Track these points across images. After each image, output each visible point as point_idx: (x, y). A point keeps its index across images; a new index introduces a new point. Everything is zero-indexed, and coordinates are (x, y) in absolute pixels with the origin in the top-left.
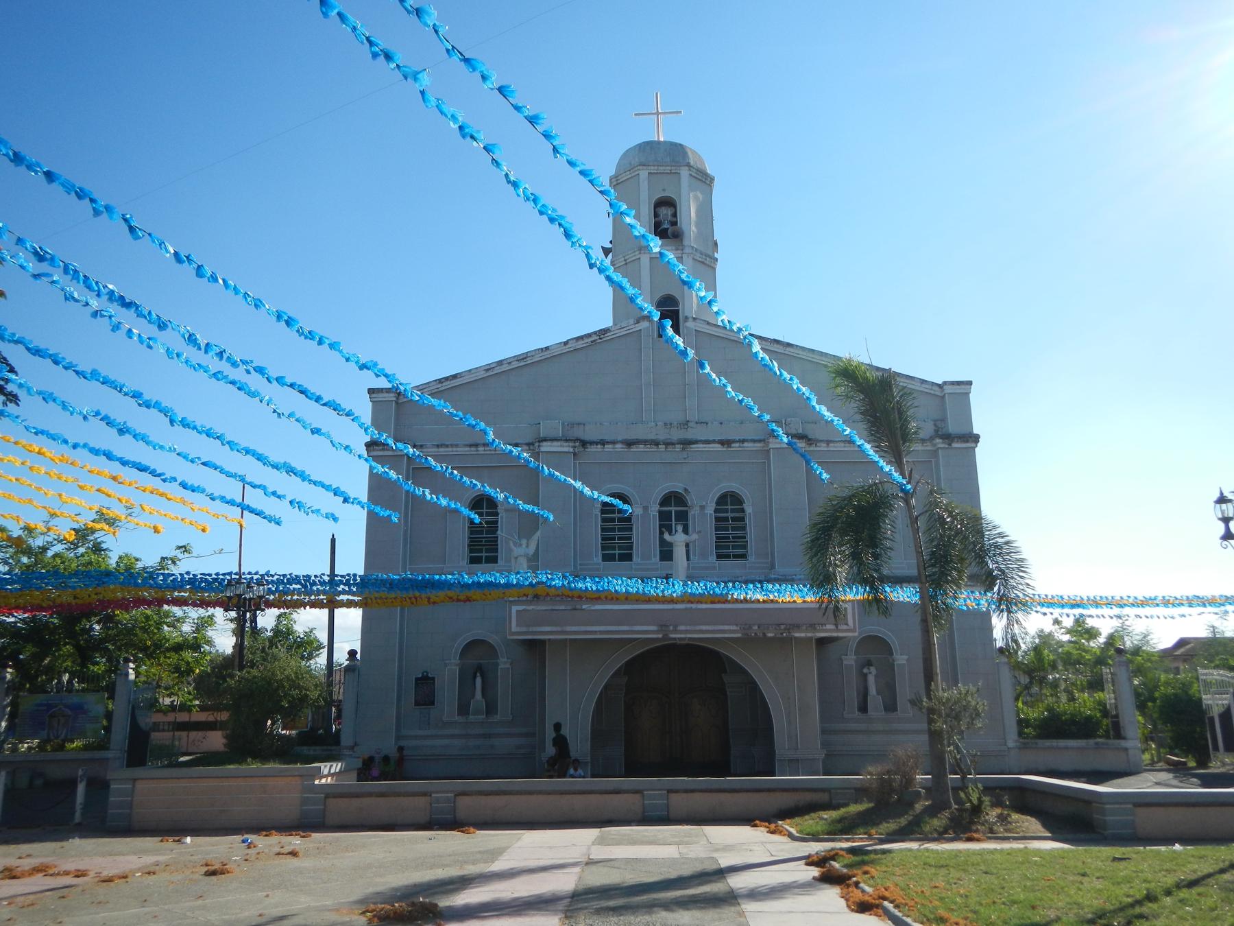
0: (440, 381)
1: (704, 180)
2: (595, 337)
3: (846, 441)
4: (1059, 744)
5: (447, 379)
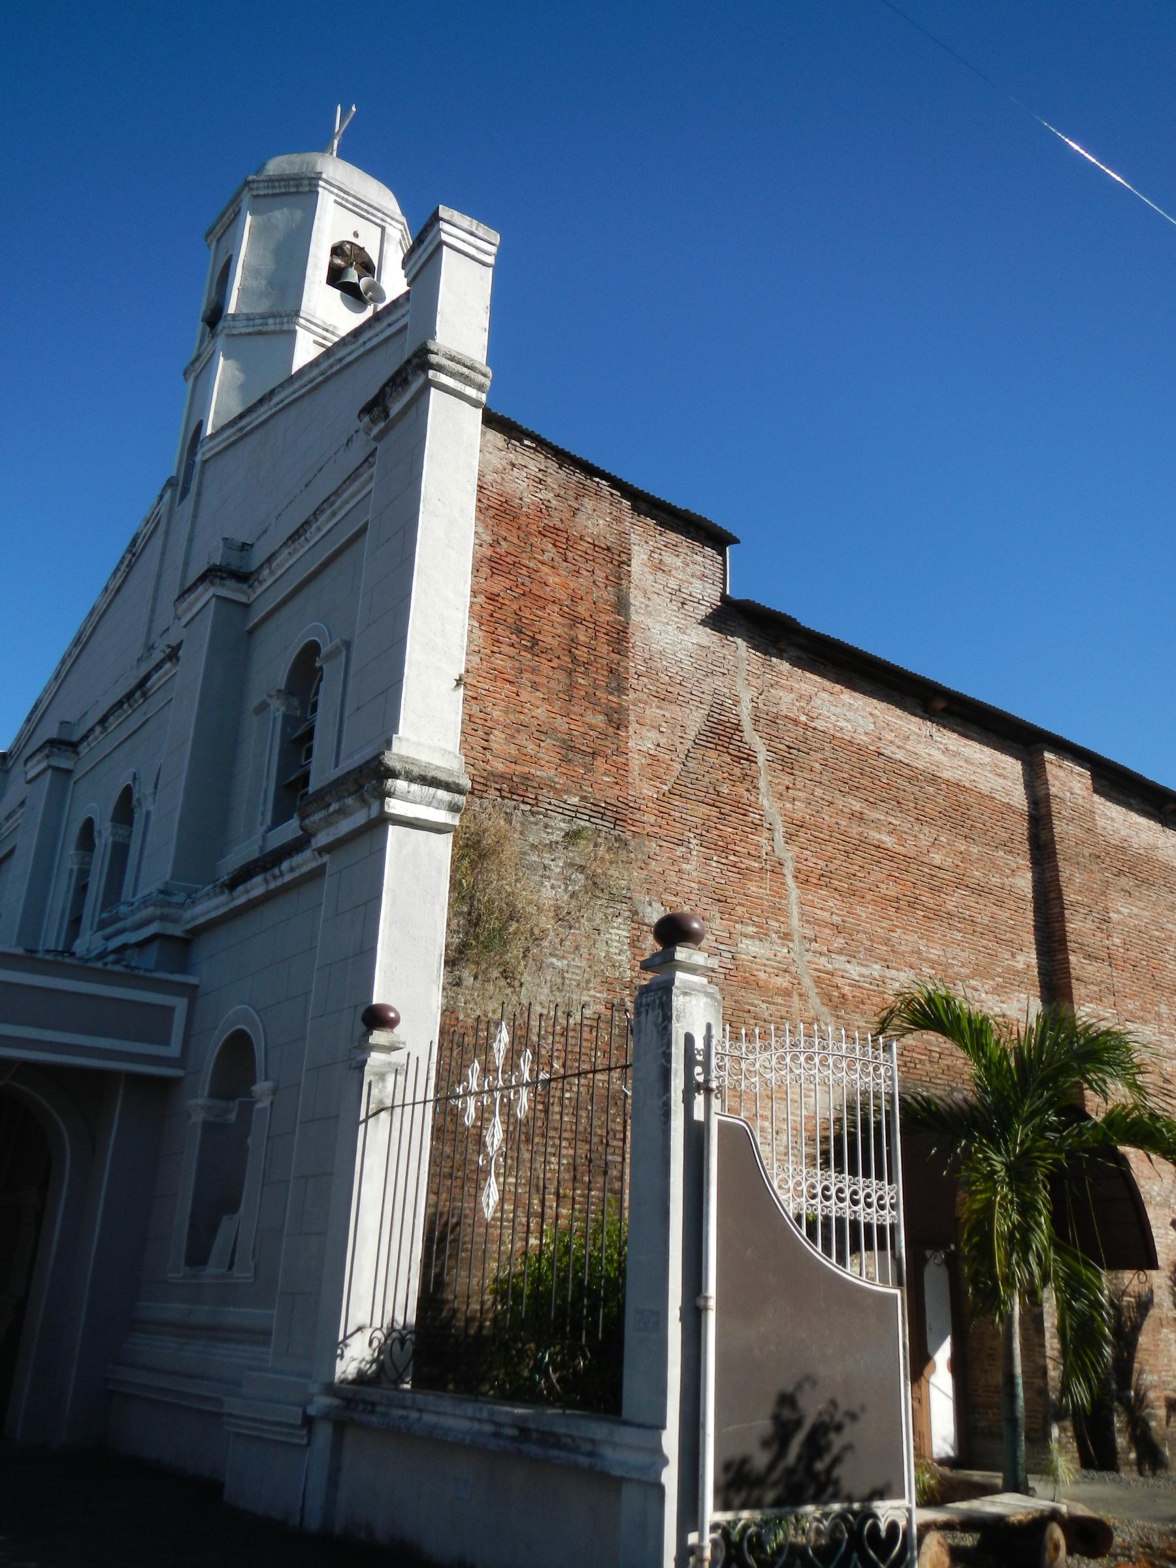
0: (29, 720)
1: (293, 190)
2: (129, 556)
3: (287, 540)
4: (427, 1417)
5: (33, 712)
